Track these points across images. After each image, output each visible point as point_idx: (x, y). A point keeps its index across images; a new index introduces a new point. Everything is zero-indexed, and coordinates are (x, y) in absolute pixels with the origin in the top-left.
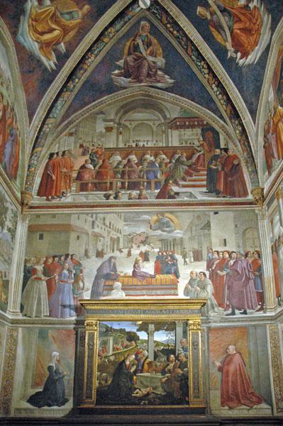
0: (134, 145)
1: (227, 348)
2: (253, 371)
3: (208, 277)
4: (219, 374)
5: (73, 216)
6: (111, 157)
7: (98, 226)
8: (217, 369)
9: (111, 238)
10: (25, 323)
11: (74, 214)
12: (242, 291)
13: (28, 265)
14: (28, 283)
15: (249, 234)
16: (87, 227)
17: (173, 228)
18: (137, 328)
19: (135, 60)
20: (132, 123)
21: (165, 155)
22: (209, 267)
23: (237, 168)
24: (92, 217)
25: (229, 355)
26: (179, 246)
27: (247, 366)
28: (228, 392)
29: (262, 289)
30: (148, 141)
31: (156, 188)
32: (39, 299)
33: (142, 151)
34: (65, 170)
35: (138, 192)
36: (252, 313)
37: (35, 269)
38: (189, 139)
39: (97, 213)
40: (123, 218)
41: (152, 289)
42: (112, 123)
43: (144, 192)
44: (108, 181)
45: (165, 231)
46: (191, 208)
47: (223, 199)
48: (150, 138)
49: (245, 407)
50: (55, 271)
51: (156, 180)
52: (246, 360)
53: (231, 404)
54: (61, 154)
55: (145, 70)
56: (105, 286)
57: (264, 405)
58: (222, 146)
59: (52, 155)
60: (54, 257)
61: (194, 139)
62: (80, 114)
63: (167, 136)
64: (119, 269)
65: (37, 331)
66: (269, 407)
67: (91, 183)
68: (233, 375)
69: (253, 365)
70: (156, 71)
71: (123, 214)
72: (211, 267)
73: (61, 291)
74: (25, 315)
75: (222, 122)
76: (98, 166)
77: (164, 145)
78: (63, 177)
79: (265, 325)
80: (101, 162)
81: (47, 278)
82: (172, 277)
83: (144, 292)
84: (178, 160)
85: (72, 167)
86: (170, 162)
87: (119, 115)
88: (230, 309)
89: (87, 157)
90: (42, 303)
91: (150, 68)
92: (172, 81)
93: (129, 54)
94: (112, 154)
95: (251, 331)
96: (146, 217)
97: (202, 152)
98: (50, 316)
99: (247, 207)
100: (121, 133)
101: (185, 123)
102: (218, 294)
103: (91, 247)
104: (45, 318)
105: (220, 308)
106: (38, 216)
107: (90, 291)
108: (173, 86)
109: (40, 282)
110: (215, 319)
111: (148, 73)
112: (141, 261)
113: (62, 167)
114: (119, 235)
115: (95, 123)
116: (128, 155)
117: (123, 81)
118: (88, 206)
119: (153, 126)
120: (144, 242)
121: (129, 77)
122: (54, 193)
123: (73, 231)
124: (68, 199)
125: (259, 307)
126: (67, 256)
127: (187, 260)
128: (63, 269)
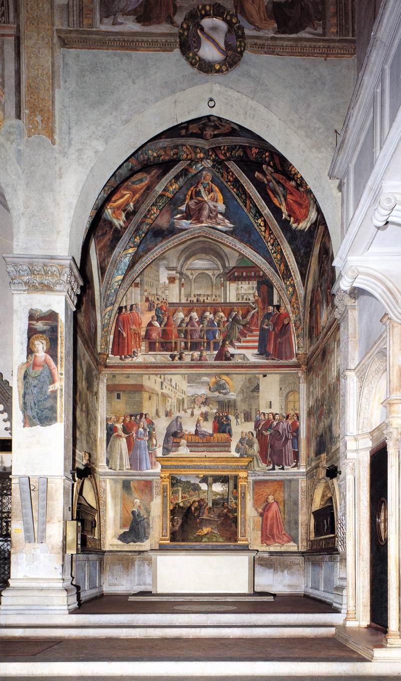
3: (255, 436)
6: (174, 314)
7: (166, 387)
12: (282, 450)
13: (110, 423)
14: (111, 440)
15: (291, 398)
16: (157, 388)
17: (228, 390)
18: (200, 480)
19: (197, 204)
21: (224, 313)
22: (256, 427)
24: (160, 378)
25: (269, 503)
26: (233, 408)
29: (298, 449)
30: (208, 295)
31: (215, 349)
33: (202, 307)
34: (134, 327)
35: (199, 353)
36: (288, 469)
37: (116, 427)
38: (245, 294)
39: (164, 374)
40: (186, 379)
42: (174, 272)
43: (204, 353)
44: (173, 341)
45: (222, 393)
46: (243, 370)
47: (271, 361)
49: (277, 544)
51: (214, 340)
53: (268, 542)
54: (128, 309)
56: (173, 443)
57: (292, 544)
58: (275, 302)
59: (120, 309)
60: (131, 416)
64: (184, 428)
66: (295, 544)
67: (158, 342)
68: (271, 519)
70: (217, 215)
71: (186, 376)
74: (111, 469)
76: (164, 324)
77: (222, 301)
79: (297, 480)
81: (126, 436)
82: (226, 435)
86: (228, 321)
88: (272, 465)
91: (211, 211)
93: (191, 198)
94: (176, 310)
96: (205, 379)
97: (256, 309)
98: (131, 469)
99: (293, 371)
104: (127, 471)
110: (259, 473)
111: (209, 216)
112: (202, 421)
114: (183, 396)
115: (158, 271)
116: (190, 311)
117: (184, 223)
118: (156, 367)
119: (212, 277)
120: (205, 403)
123: (146, 391)
125: (294, 464)
126: (141, 415)
128: (139, 427)
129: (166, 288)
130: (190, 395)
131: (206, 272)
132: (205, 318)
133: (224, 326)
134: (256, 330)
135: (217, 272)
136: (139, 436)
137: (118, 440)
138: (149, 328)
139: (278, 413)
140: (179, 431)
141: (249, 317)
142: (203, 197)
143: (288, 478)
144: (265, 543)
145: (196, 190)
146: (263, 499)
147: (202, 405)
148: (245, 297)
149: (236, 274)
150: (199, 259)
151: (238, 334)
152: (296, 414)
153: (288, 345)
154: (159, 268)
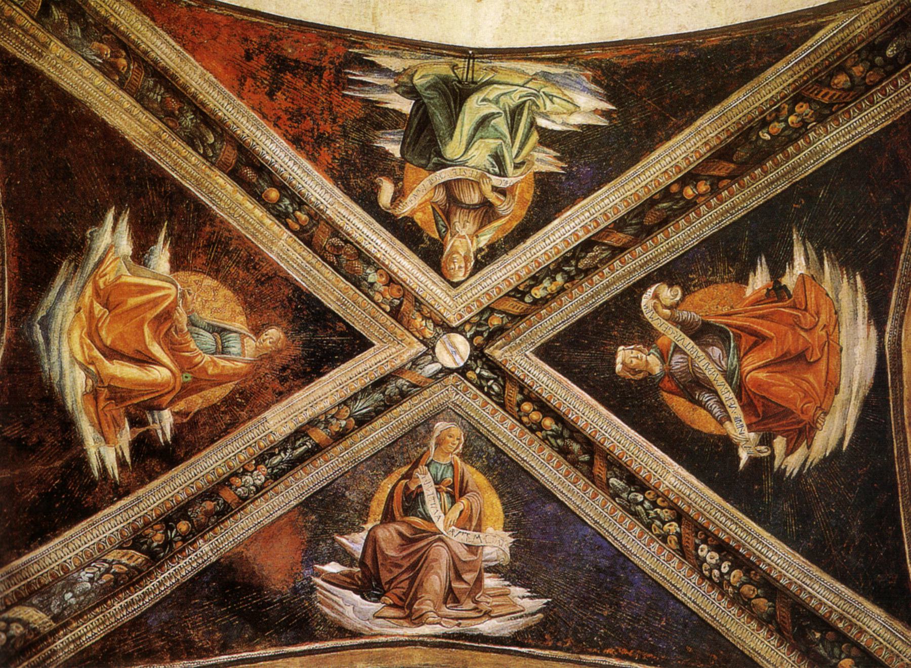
19: (408, 541)
70: (479, 580)
92: (540, 603)
93: (388, 517)
108: (542, 623)
111: (450, 590)
121: (378, 598)
142: (428, 518)
145: (407, 487)
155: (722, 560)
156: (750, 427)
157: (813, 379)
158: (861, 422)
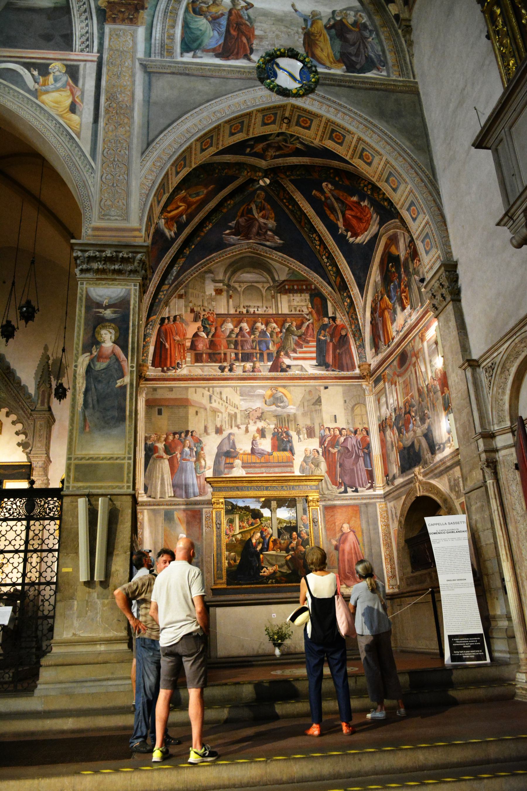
0: (245, 311)
1: (342, 527)
2: (366, 550)
3: (321, 454)
4: (335, 553)
5: (190, 390)
8: (333, 548)
9: (229, 414)
10: (150, 505)
11: (191, 387)
12: (353, 469)
13: (149, 443)
15: (357, 411)
16: (205, 401)
19: (247, 221)
20: (242, 285)
21: (277, 324)
22: (322, 443)
23: (343, 341)
24: (209, 391)
25: (344, 534)
26: (293, 422)
27: (361, 544)
28: (344, 571)
29: (371, 467)
30: (258, 307)
31: (269, 360)
32: (163, 479)
33: (253, 318)
34: (177, 338)
35: (252, 364)
36: (362, 491)
37: (157, 447)
38: (298, 306)
39: (213, 387)
40: (238, 392)
41: (270, 467)
42: (221, 284)
43: (258, 364)
44: (222, 352)
45: (280, 407)
47: (332, 373)
48: (260, 304)
50: (176, 448)
51: (268, 351)
52: (360, 539)
54: (172, 319)
55: (255, 230)
56: (226, 463)
58: (330, 314)
59: (163, 320)
60: (175, 434)
61: (303, 306)
62: (190, 273)
63: (276, 302)
65: (163, 513)
67: (206, 353)
69: (366, 544)
70: (266, 232)
71: (238, 388)
72: (323, 444)
73: (183, 470)
74: (150, 497)
75: (330, 289)
78: (176, 346)
79: (374, 504)
80: (213, 330)
81: (169, 457)
82: (287, 454)
83: (263, 470)
84: (288, 330)
85: (184, 335)
86: (281, 332)
87: (228, 275)
88: (343, 487)
89: (199, 324)
90: (166, 483)
91: (260, 227)
93: (242, 216)
94: (224, 322)
95: (363, 509)
96: (261, 391)
98: (174, 496)
100: (231, 297)
101: (293, 286)
102: (331, 471)
103: (209, 421)
105: (334, 486)
106: (155, 389)
107: (212, 470)
109: (162, 460)
110: (329, 497)
113: (174, 334)
114: (236, 410)
115: (204, 283)
116: (240, 322)
117: (233, 238)
119: (262, 289)
120: (260, 418)
122: (169, 366)
123: (192, 405)
124: (184, 371)
125: (369, 485)
126: (187, 432)
127: (301, 436)
128: (184, 447)
129: (212, 299)
130: (244, 409)
131: (255, 284)
132: (256, 329)
133: (277, 337)
134: (313, 341)
135: (266, 286)
136: (184, 457)
137: (158, 462)
138: (194, 339)
139: (344, 427)
140: (232, 450)
141: (304, 329)
142: (253, 215)
143: (364, 501)
144: (345, 584)
146: (337, 529)
147: (258, 421)
148: (298, 309)
149: (287, 287)
150: (248, 272)
151: (293, 346)
152: (365, 428)
153: (348, 356)
154: (204, 280)
155: (328, 262)
156: (344, 226)
157: (362, 226)
158: (369, 241)
